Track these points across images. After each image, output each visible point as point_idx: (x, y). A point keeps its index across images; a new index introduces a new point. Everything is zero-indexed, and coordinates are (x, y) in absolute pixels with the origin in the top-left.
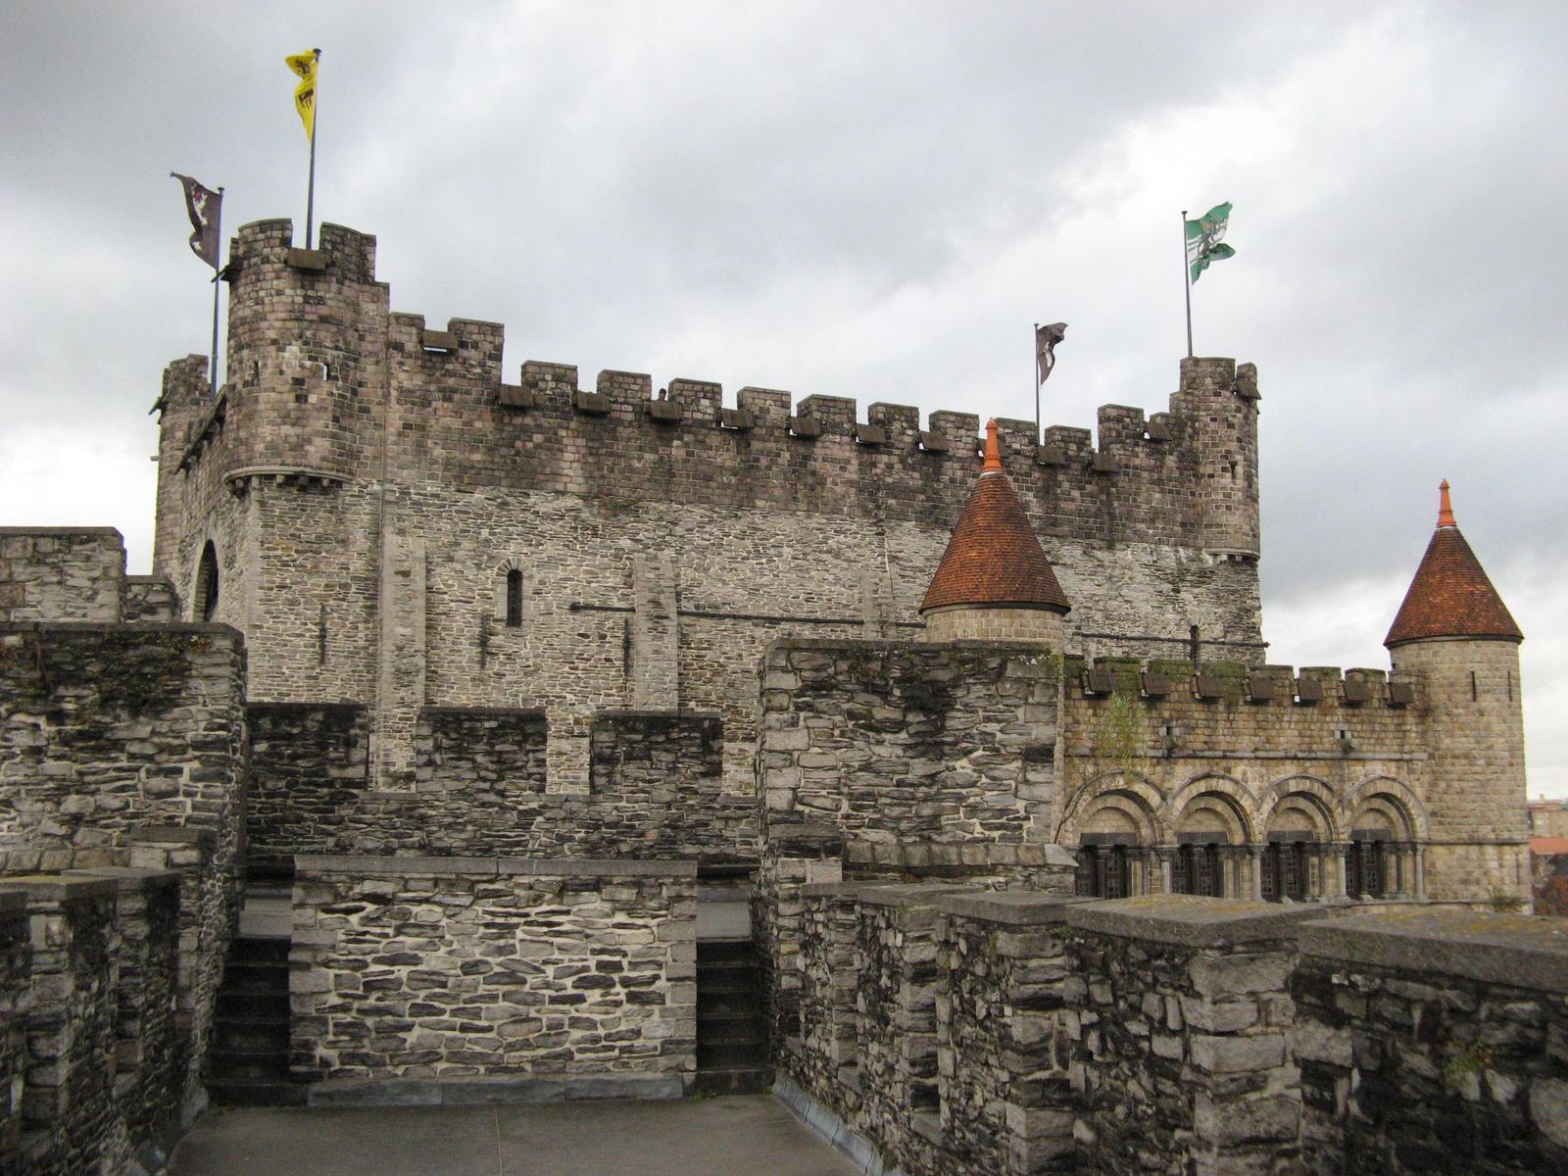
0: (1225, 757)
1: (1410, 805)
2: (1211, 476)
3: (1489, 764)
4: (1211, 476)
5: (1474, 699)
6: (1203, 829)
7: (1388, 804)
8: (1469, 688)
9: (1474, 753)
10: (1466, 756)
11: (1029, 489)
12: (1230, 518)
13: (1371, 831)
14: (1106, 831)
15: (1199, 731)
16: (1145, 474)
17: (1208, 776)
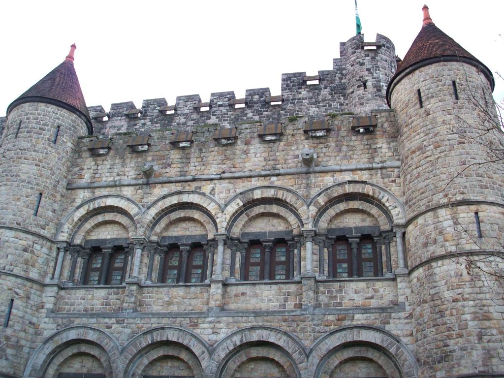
0: (194, 180)
1: (384, 200)
2: (352, 92)
3: (436, 148)
4: (352, 92)
5: (421, 106)
6: (188, 233)
7: (367, 204)
8: (417, 101)
9: (425, 143)
10: (419, 149)
11: (224, 120)
12: (362, 109)
13: (356, 228)
14: (109, 237)
15: (173, 166)
16: (306, 101)
17: (179, 193)
